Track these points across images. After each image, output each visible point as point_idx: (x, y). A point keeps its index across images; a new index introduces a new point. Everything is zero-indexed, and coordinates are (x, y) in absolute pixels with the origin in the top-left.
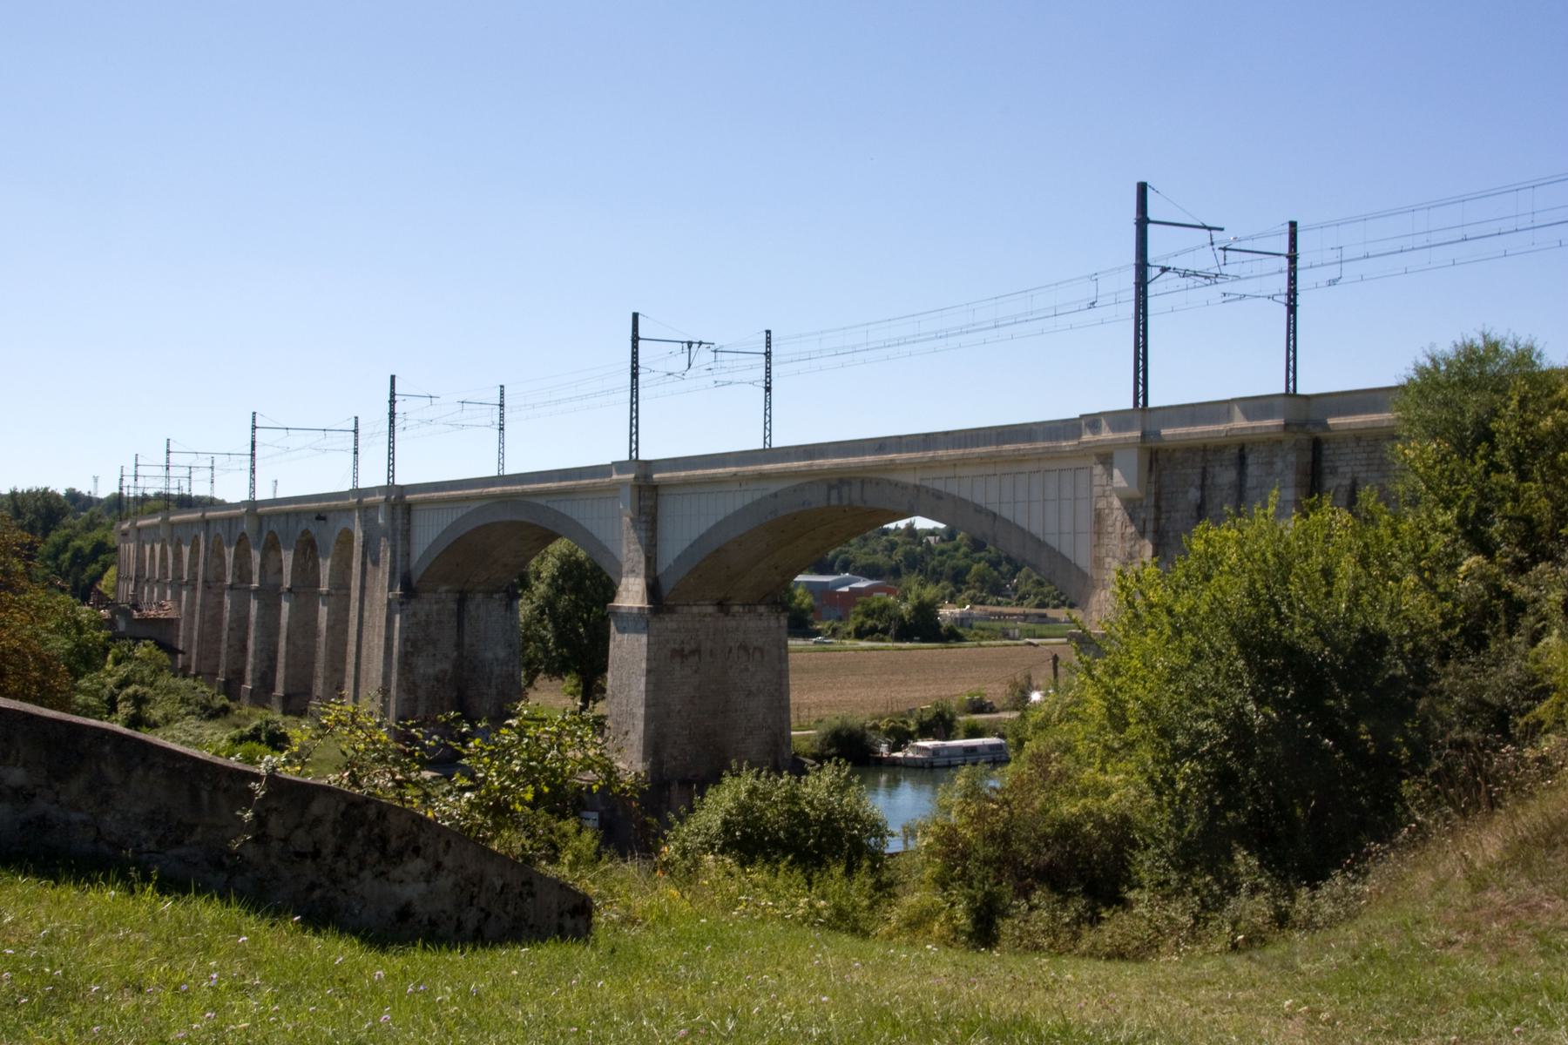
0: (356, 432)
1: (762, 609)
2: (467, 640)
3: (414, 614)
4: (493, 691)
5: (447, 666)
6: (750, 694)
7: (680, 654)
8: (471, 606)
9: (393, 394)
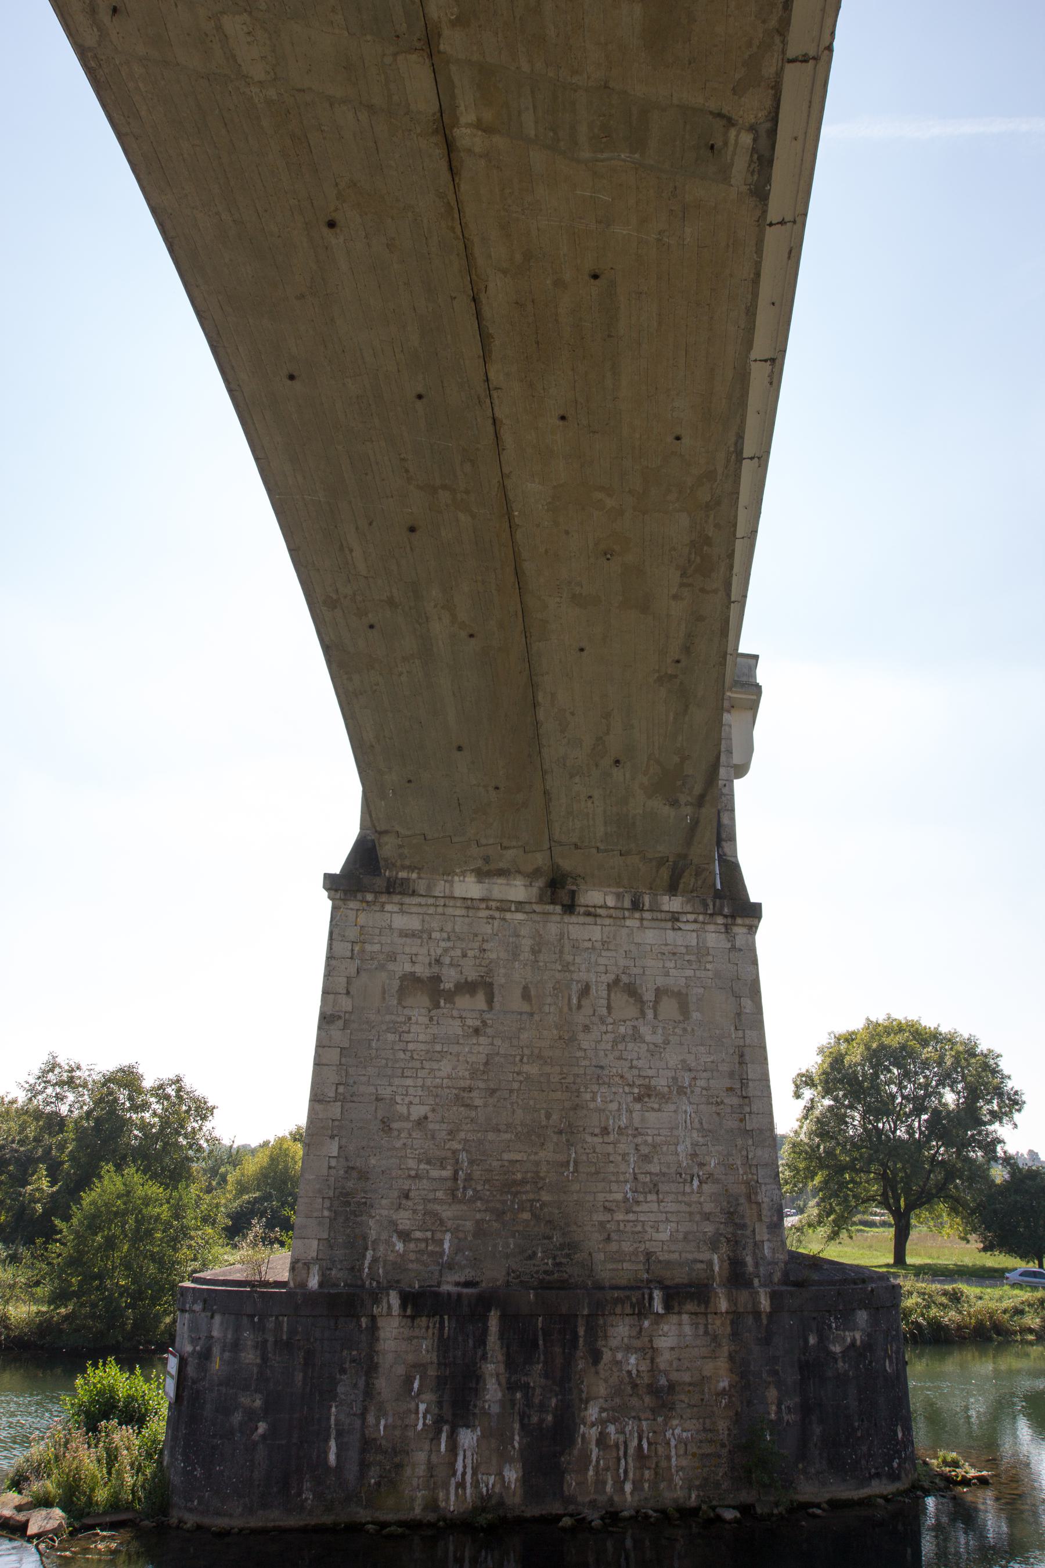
1: (673, 904)
6: (646, 1094)
7: (433, 989)
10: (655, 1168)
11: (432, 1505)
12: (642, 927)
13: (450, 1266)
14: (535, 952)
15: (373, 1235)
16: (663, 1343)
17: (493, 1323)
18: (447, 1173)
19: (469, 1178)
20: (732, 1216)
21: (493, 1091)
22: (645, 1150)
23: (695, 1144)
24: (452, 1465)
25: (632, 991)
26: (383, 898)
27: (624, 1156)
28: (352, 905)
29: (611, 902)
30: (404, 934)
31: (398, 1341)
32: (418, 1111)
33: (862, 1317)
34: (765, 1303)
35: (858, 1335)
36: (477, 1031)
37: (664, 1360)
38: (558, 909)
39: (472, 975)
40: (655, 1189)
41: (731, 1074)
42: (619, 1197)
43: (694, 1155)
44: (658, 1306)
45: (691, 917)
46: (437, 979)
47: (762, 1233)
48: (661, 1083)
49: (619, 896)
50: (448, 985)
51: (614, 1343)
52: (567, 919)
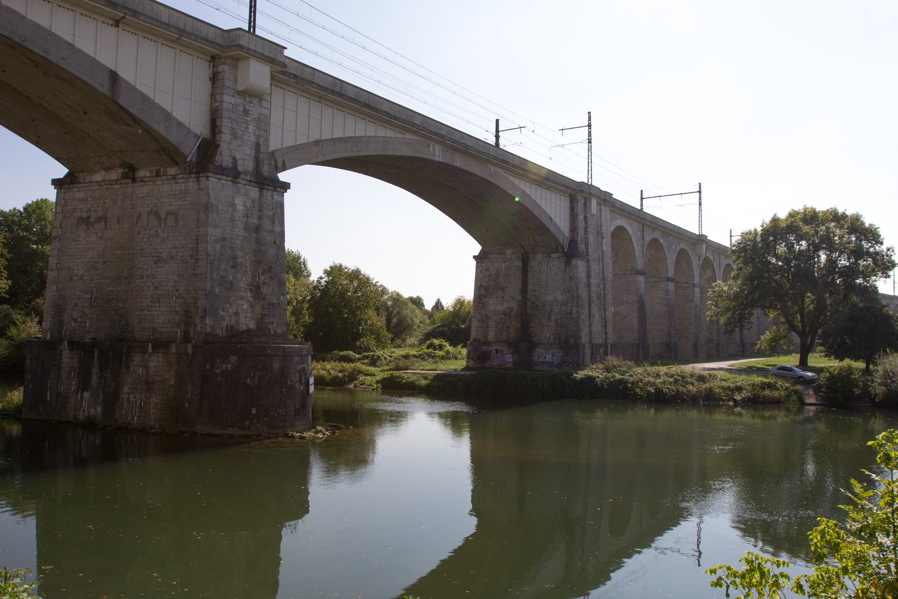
0: (700, 192)
1: (172, 171)
2: (530, 287)
3: (487, 270)
4: (553, 324)
5: (513, 304)
6: (159, 260)
8: (534, 264)
9: (497, 131)
10: (159, 292)
11: (75, 417)
12: (163, 184)
13: (88, 332)
14: (122, 201)
15: (66, 320)
16: (152, 364)
17: (96, 353)
18: (89, 296)
19: (96, 298)
20: (187, 314)
21: (105, 263)
22: (156, 285)
23: (175, 281)
24: (82, 404)
25: (157, 214)
26: (71, 186)
27: (149, 287)
28: (63, 190)
29: (148, 175)
30: (79, 200)
31: (68, 359)
32: (81, 272)
33: (233, 359)
34: (190, 350)
35: (229, 367)
36: (101, 238)
37: (152, 370)
38: (130, 180)
39: (100, 214)
40: (159, 301)
41: (193, 248)
42: (145, 304)
43: (175, 286)
44: (150, 350)
45: (181, 176)
46: (89, 217)
47: (197, 320)
48: (164, 255)
49: (151, 171)
50: (92, 220)
51: (135, 363)
52: (135, 184)
